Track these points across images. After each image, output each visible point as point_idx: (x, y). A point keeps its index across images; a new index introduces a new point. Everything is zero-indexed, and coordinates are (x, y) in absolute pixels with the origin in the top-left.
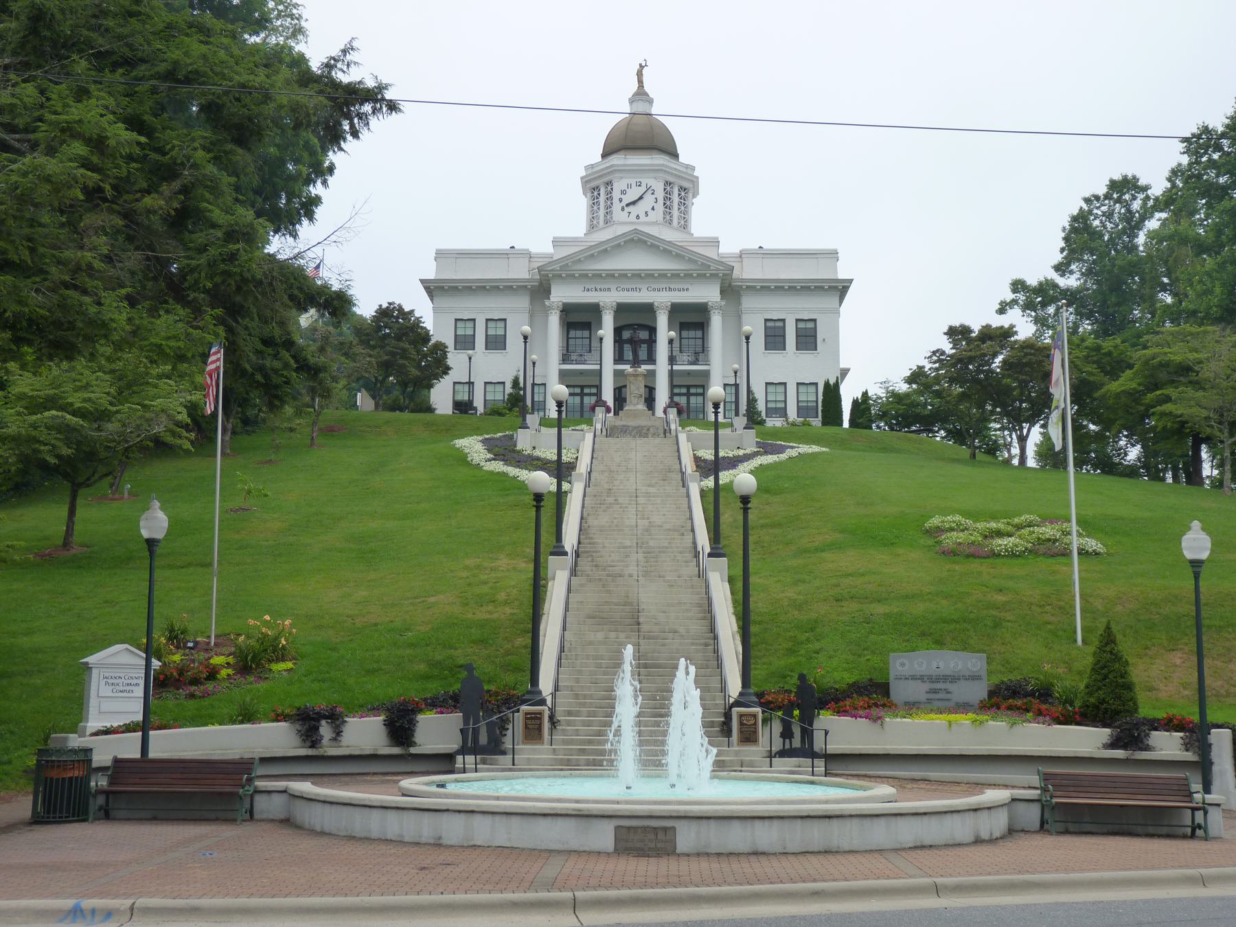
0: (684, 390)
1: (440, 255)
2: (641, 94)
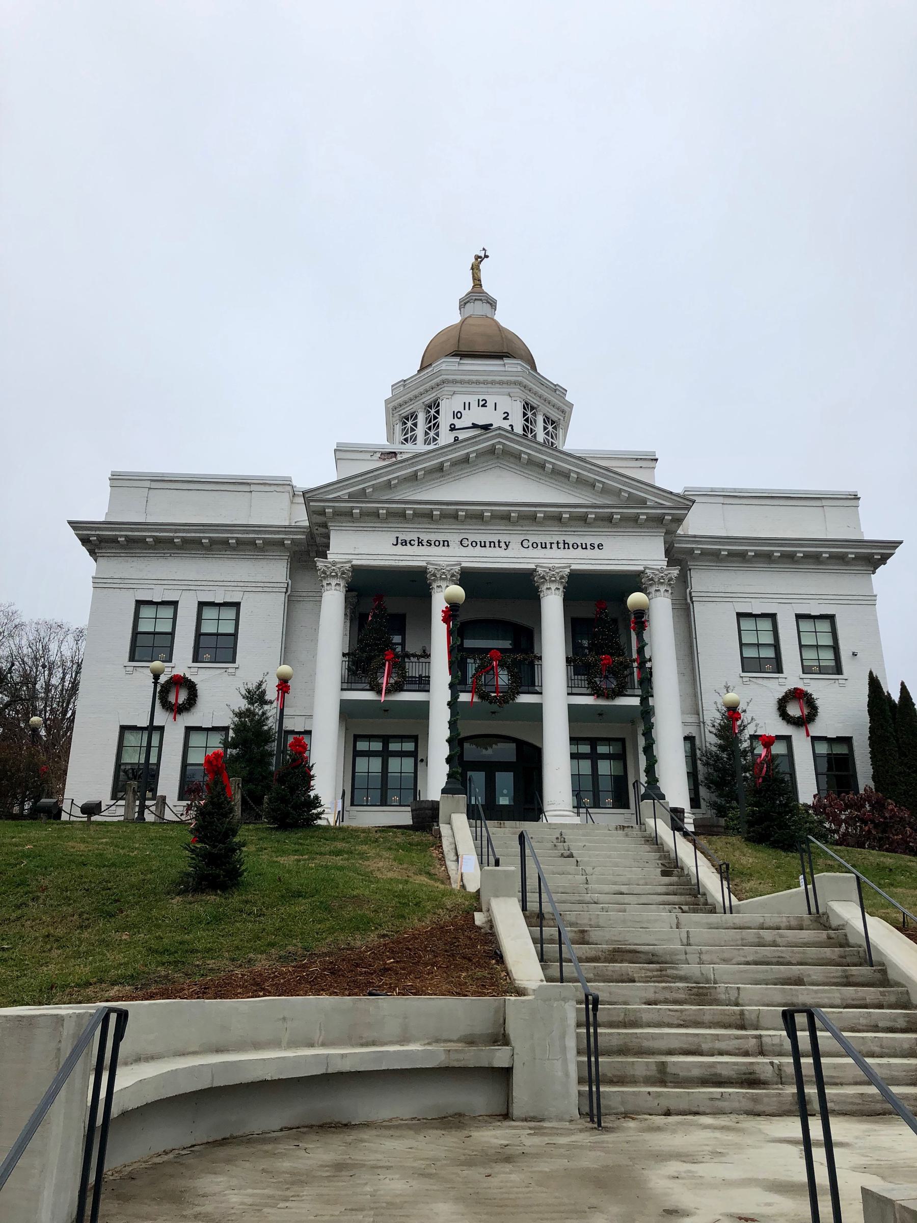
1: (117, 479)
2: (477, 295)
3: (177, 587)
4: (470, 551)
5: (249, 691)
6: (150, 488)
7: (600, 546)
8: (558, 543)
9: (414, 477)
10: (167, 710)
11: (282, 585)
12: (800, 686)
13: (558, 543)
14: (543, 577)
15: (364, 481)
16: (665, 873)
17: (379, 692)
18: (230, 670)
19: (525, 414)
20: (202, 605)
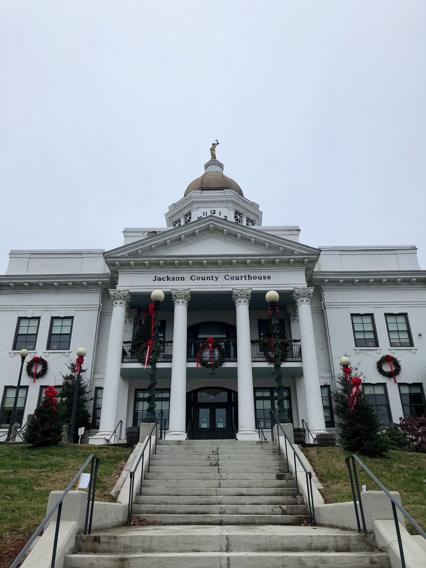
0: (267, 394)
2: (214, 161)
3: (40, 309)
4: (196, 282)
5: (72, 365)
6: (30, 258)
7: (269, 277)
8: (245, 276)
9: (164, 244)
10: (31, 376)
11: (97, 306)
12: (390, 354)
13: (245, 276)
14: (237, 295)
15: (136, 246)
16: (279, 477)
17: (144, 363)
18: (66, 354)
19: (236, 217)
20: (53, 318)
